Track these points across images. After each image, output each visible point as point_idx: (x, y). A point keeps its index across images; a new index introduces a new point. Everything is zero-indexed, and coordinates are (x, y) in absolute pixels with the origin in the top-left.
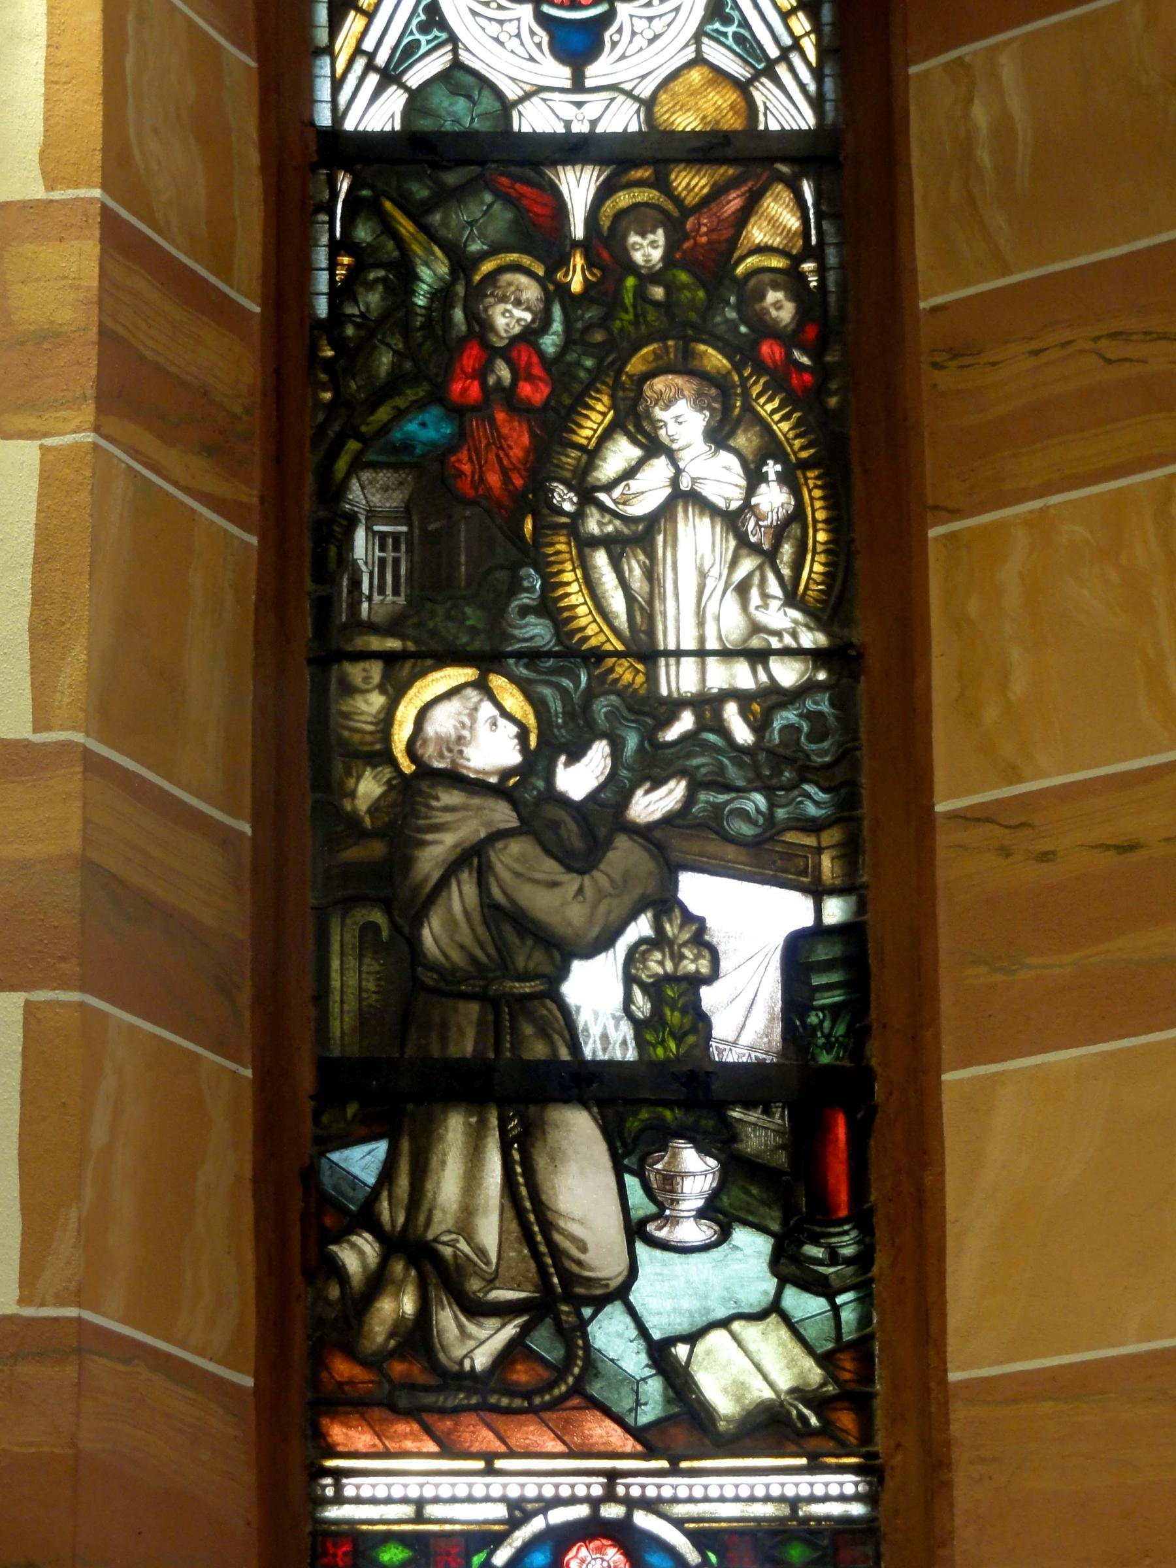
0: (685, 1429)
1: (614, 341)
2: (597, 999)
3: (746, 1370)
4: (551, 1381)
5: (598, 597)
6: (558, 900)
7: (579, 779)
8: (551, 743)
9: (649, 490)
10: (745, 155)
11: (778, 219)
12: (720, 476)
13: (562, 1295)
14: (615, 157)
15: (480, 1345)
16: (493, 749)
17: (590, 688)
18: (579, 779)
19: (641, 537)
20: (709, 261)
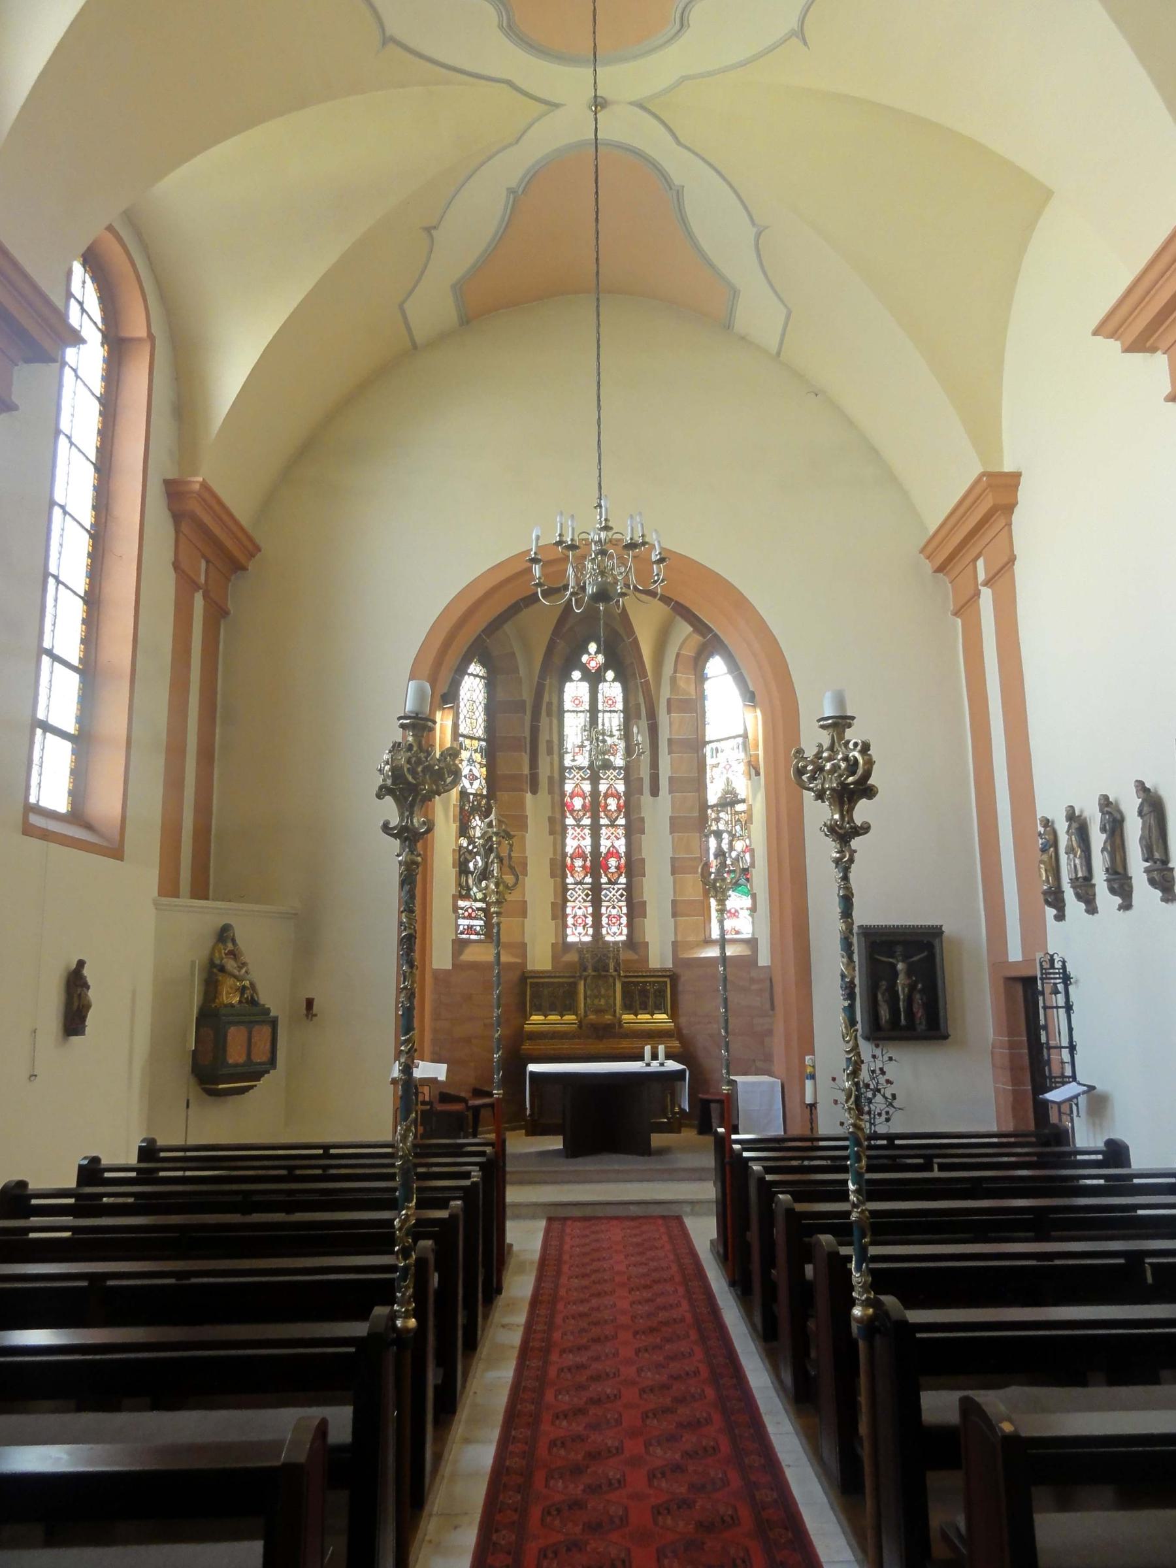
0: (476, 900)
1: (474, 810)
2: (471, 865)
3: (479, 896)
4: (467, 897)
5: (471, 832)
6: (469, 857)
7: (471, 847)
8: (469, 844)
9: (474, 824)
10: (481, 795)
11: (484, 802)
12: (479, 823)
13: (469, 889)
14: (475, 795)
15: (464, 893)
16: (465, 845)
17: (471, 841)
18: (471, 847)
19: (474, 828)
20: (479, 804)
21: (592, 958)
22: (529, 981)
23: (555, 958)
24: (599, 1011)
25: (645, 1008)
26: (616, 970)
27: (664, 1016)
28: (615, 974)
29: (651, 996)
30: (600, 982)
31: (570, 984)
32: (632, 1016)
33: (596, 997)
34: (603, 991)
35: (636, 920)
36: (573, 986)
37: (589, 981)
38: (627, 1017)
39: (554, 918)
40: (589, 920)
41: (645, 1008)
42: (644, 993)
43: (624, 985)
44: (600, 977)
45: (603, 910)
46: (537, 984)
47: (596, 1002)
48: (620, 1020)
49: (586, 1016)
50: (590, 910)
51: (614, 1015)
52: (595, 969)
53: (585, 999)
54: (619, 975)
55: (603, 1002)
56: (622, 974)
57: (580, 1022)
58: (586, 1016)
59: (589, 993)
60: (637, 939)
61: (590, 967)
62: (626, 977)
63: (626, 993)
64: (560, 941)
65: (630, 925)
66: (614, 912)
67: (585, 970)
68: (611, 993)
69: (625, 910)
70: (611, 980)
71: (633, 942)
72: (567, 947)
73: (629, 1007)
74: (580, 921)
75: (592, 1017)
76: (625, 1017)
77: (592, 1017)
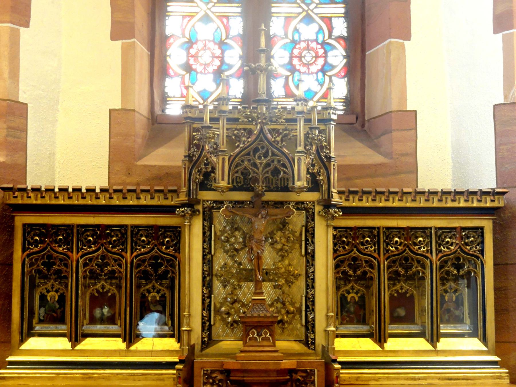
21: (232, 141)
22: (21, 220)
23: (119, 154)
24: (256, 326)
25: (409, 319)
26: (314, 185)
27: (474, 344)
28: (313, 196)
29: (431, 277)
30: (261, 224)
31: (154, 231)
32: (367, 344)
33: (248, 276)
34: (269, 258)
35: (376, 53)
36: (176, 233)
37: (220, 220)
38: (353, 346)
39: (120, 30)
40: (234, 56)
41: (403, 313)
42: (406, 268)
43: (342, 237)
44: (259, 205)
45: (276, 26)
46: (49, 232)
47: (246, 291)
48: (328, 364)
49: (208, 341)
50: (237, 26)
51: (308, 342)
52: (242, 182)
53: (207, 283)
54: (327, 205)
55: (268, 292)
56: (336, 199)
57: (188, 362)
58: (208, 341)
59: (220, 260)
60: (375, 107)
61: (221, 164)
62: (348, 211)
63: (350, 269)
64: (142, 106)
65: (357, 68)
66: (309, 32)
67: (206, 182)
68: (296, 262)
69: (340, 27)
70: (298, 220)
71: (359, 120)
72: (159, 128)
73: (353, 313)
74: (205, 57)
75: (229, 344)
76: (341, 344)
77: (229, 344)
